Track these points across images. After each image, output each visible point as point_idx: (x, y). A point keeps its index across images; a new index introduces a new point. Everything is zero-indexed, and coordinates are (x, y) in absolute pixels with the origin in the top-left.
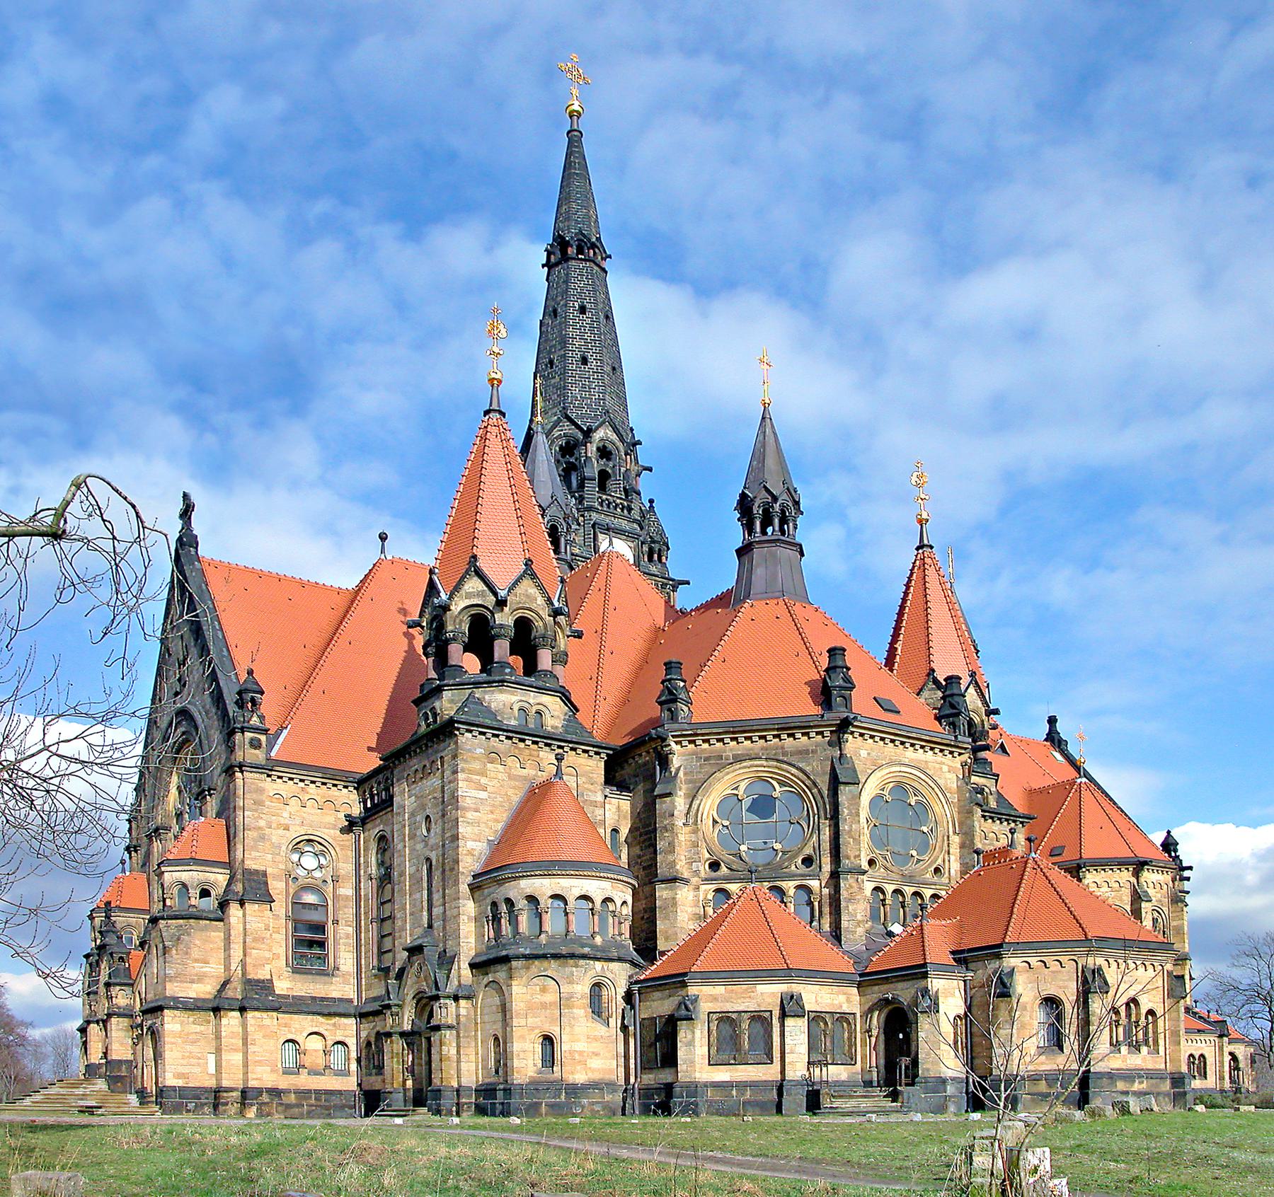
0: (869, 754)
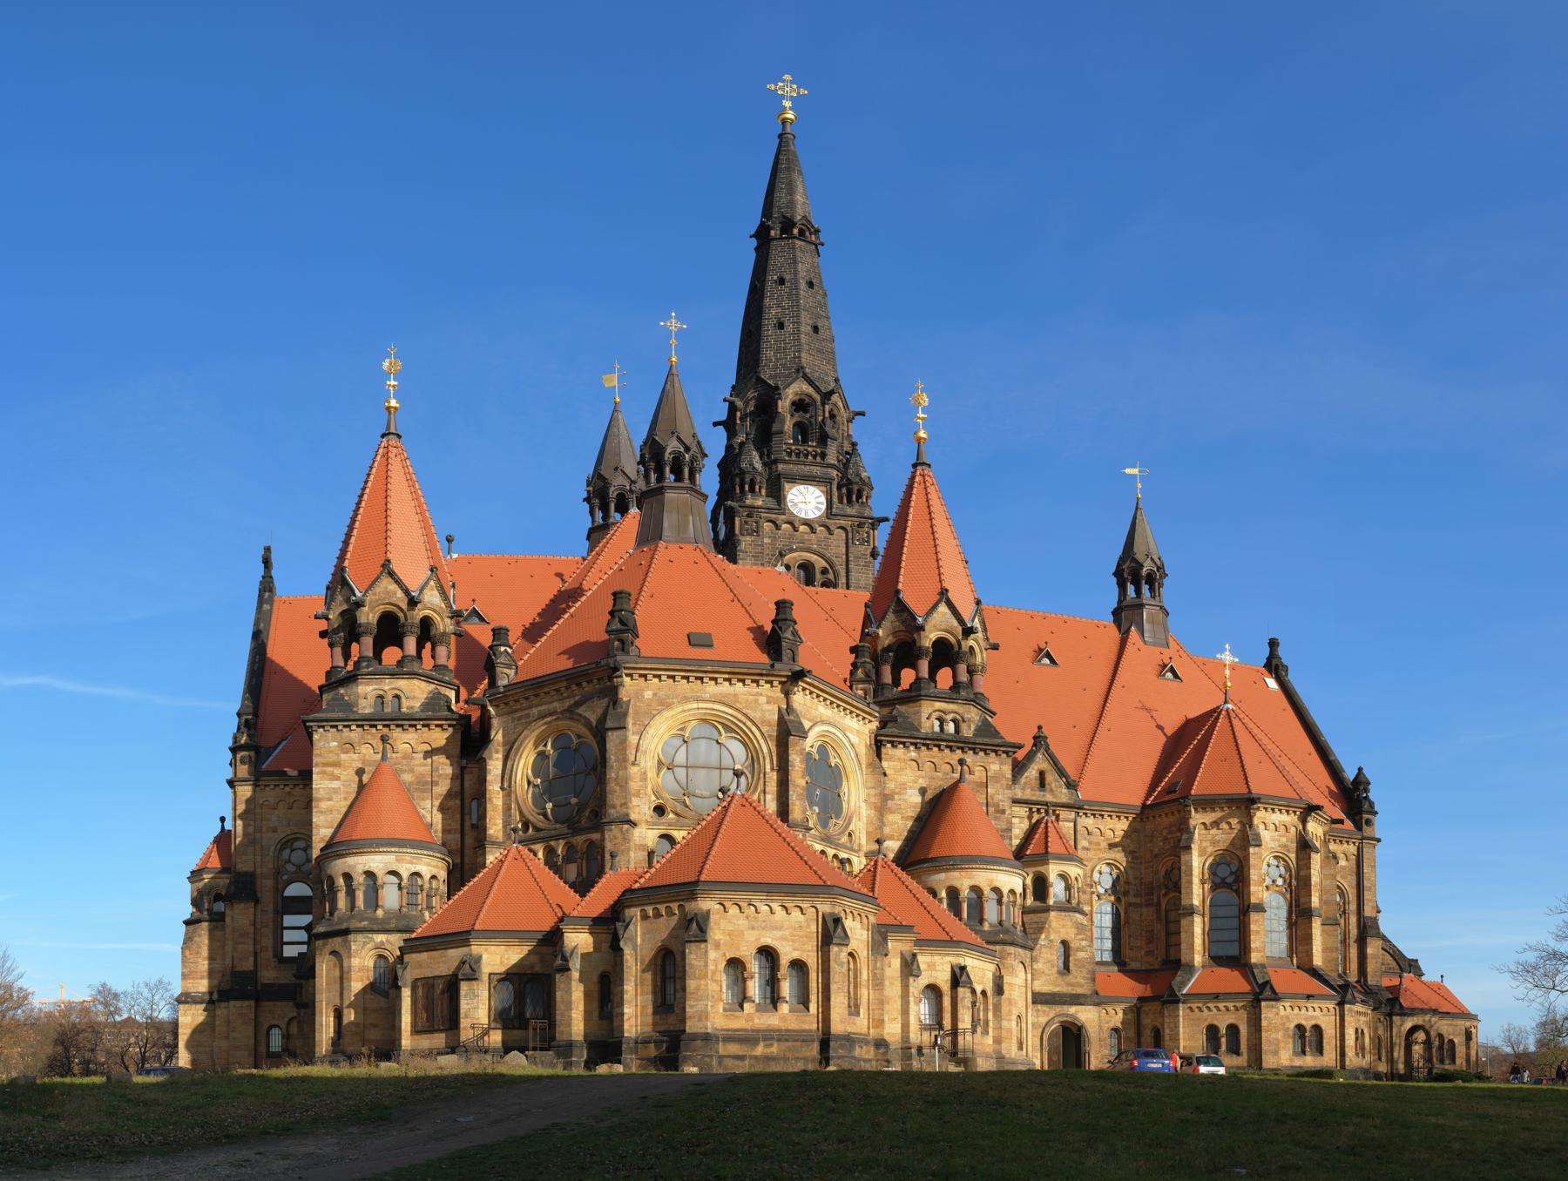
0: (655, 694)
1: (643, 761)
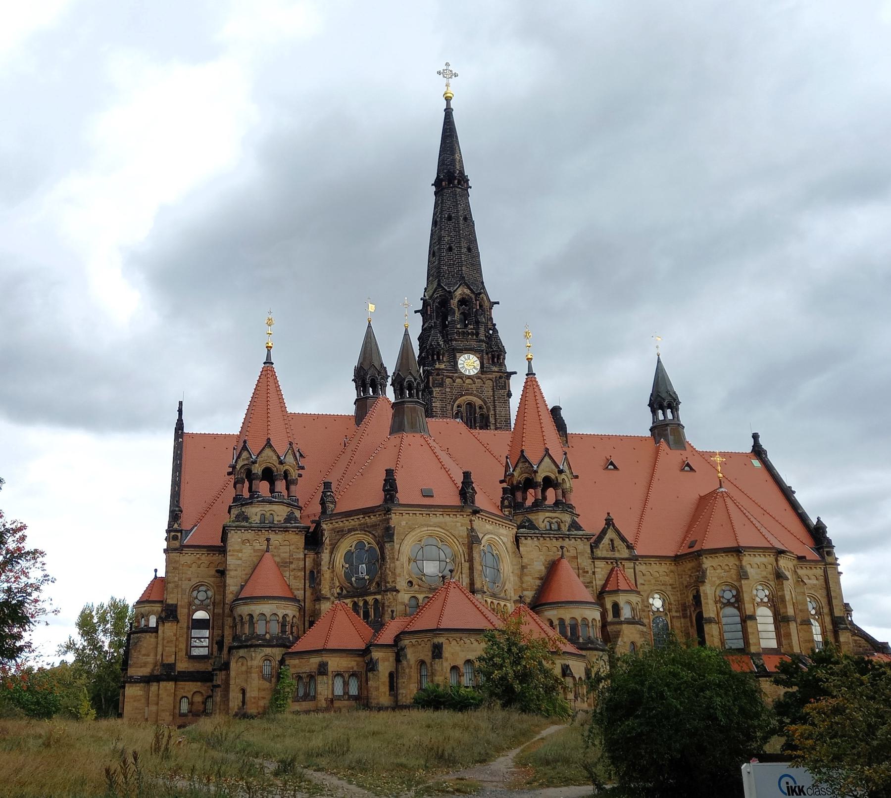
0: (407, 523)
1: (402, 558)
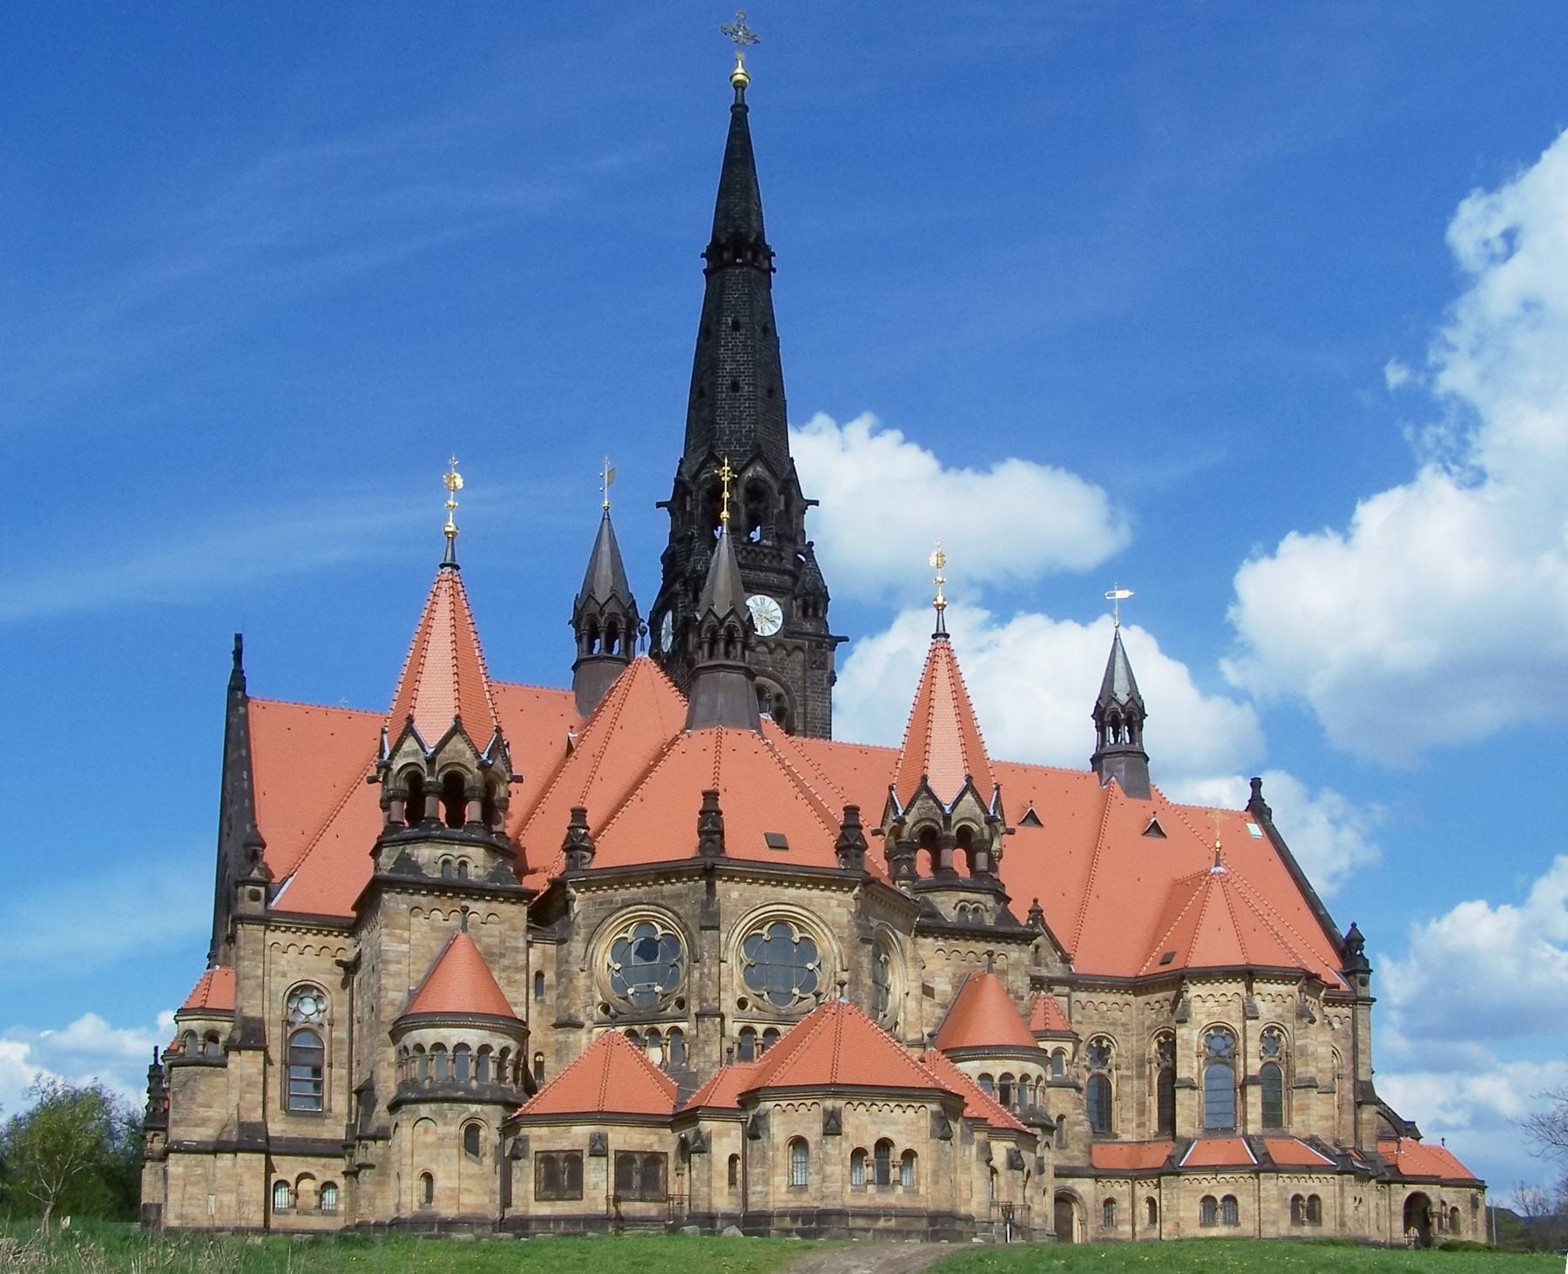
0: (741, 895)
